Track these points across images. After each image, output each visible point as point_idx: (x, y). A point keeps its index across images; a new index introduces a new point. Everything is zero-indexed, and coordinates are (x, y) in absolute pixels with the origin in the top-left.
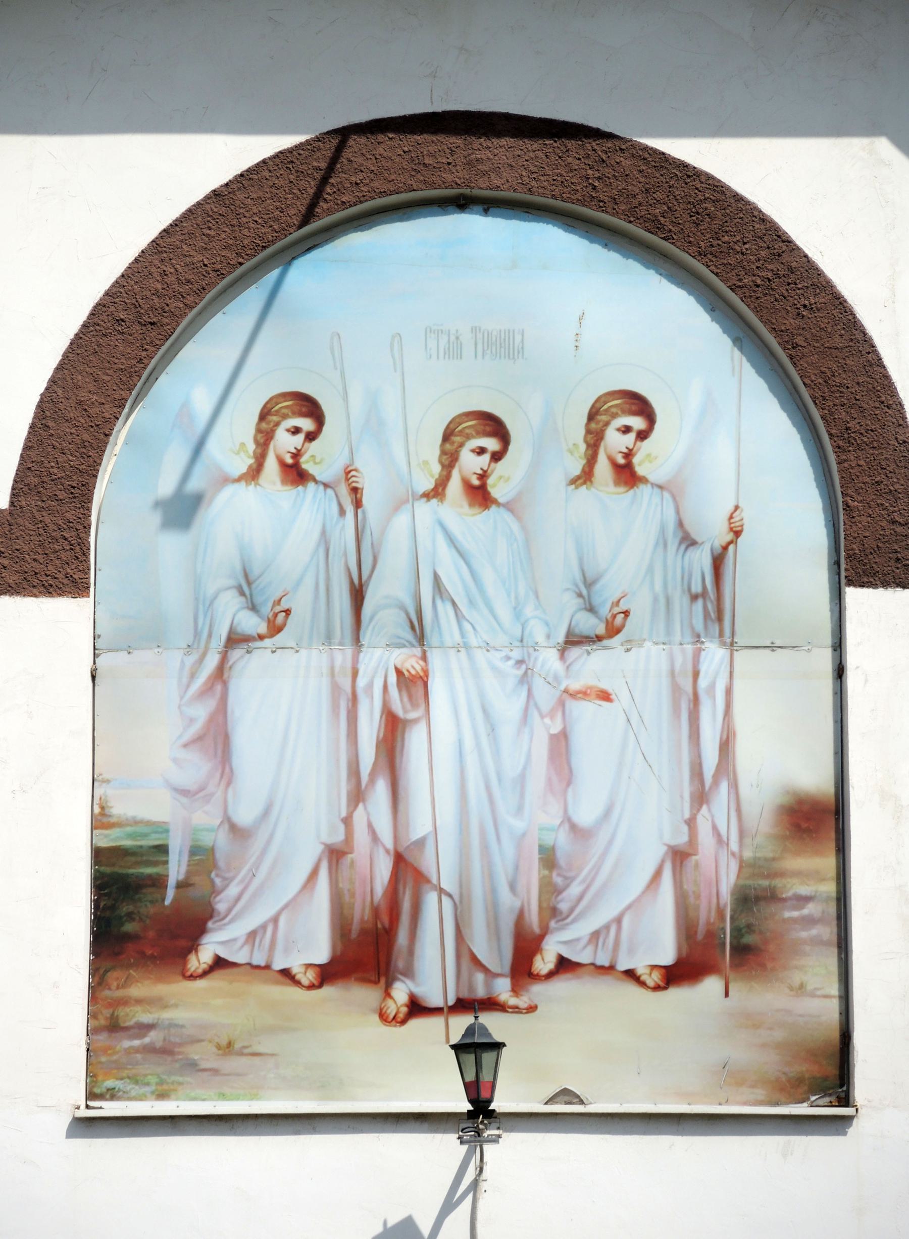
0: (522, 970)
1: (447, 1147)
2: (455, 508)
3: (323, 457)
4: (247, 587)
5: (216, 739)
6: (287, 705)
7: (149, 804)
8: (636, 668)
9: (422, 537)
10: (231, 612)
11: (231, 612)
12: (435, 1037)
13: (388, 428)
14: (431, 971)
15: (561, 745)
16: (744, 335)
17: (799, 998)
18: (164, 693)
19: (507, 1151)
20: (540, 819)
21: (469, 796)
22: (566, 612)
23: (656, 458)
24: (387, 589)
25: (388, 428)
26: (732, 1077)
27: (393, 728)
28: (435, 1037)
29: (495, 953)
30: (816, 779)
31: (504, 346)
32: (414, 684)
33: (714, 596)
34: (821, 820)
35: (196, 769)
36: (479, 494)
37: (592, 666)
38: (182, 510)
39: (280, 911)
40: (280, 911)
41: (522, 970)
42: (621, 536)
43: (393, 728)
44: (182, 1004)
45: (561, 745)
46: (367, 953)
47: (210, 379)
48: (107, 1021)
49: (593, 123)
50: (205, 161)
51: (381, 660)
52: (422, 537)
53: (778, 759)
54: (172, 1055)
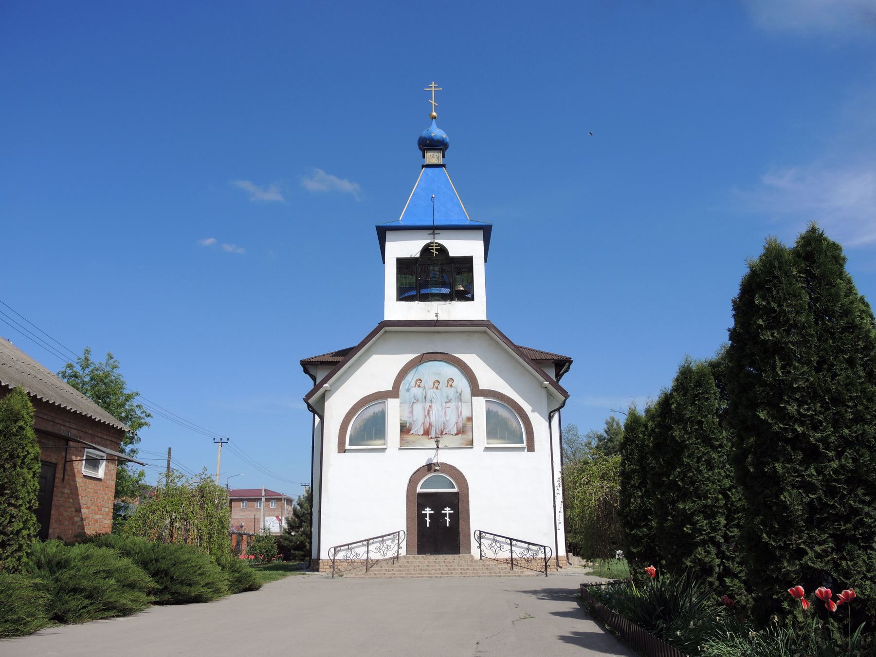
0: (442, 434)
1: (435, 451)
2: (435, 390)
3: (422, 385)
4: (414, 397)
5: (412, 412)
6: (418, 409)
7: (405, 419)
8: (452, 405)
9: (431, 392)
10: (413, 400)
11: (413, 400)
12: (433, 441)
13: (428, 381)
14: (433, 435)
15: (445, 412)
16: (462, 373)
17: (468, 436)
18: (407, 407)
19: (440, 451)
20: (443, 419)
21: (436, 417)
22: (445, 399)
23: (454, 384)
24: (428, 397)
25: (428, 381)
26: (462, 444)
27: (429, 411)
28: (433, 441)
29: (439, 433)
30: (470, 415)
31: (439, 374)
32: (431, 407)
33: (460, 398)
34: (470, 419)
35: (410, 415)
36: (437, 388)
37: (448, 405)
38: (408, 390)
39: (418, 429)
40: (418, 429)
41: (442, 434)
42: (451, 392)
43: (429, 411)
44: (409, 438)
45: (445, 412)
46: (427, 433)
47: (411, 378)
48: (402, 439)
49: (558, 617)
50: (411, 357)
51: (428, 404)
52: (431, 392)
53: (466, 413)
54: (408, 443)
